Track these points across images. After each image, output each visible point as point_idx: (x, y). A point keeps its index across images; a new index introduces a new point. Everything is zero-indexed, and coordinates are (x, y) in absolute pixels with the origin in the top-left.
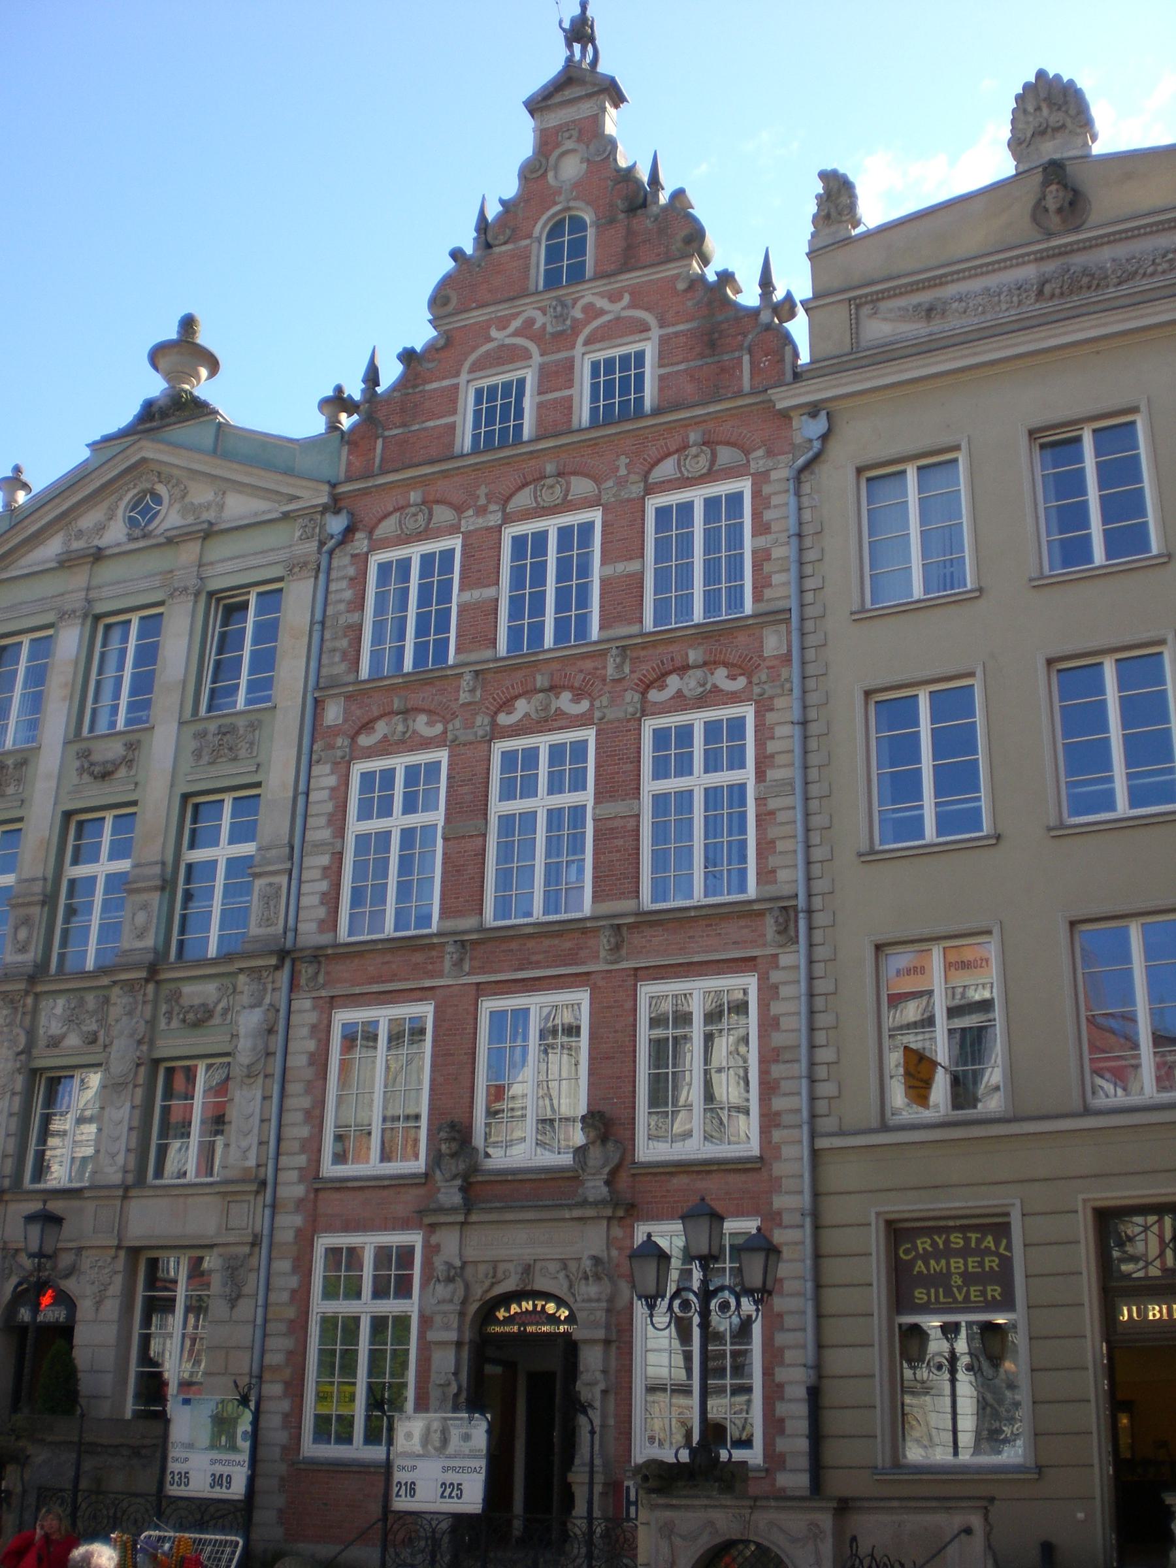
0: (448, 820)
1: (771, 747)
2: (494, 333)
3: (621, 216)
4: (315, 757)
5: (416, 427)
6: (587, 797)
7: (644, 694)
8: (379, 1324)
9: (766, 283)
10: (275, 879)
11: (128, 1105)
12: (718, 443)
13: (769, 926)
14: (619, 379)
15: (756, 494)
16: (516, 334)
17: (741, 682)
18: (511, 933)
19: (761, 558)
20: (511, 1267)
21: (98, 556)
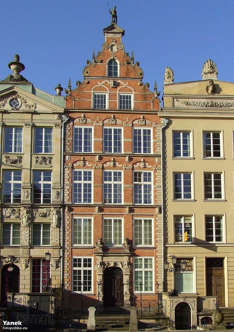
0: (94, 183)
1: (156, 179)
2: (98, 83)
3: (126, 64)
4: (65, 167)
5: (82, 100)
6: (122, 182)
7: (133, 165)
8: (85, 272)
9: (156, 89)
10: (58, 190)
11: (28, 231)
12: (146, 119)
13: (157, 210)
14: (125, 101)
15: (154, 131)
16: (103, 84)
17: (151, 166)
18: (109, 206)
19: (155, 143)
20: (111, 263)
21: (6, 112)
